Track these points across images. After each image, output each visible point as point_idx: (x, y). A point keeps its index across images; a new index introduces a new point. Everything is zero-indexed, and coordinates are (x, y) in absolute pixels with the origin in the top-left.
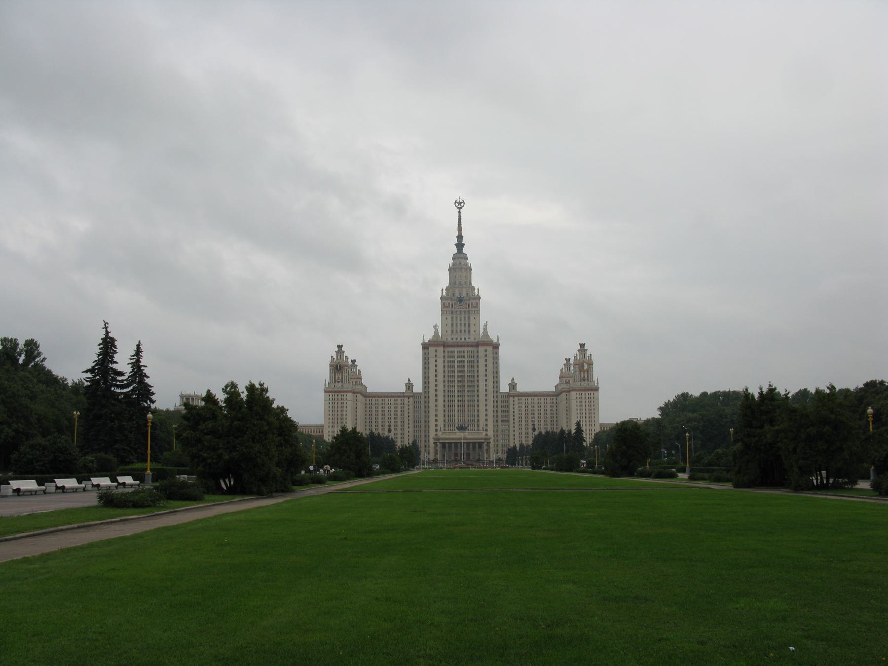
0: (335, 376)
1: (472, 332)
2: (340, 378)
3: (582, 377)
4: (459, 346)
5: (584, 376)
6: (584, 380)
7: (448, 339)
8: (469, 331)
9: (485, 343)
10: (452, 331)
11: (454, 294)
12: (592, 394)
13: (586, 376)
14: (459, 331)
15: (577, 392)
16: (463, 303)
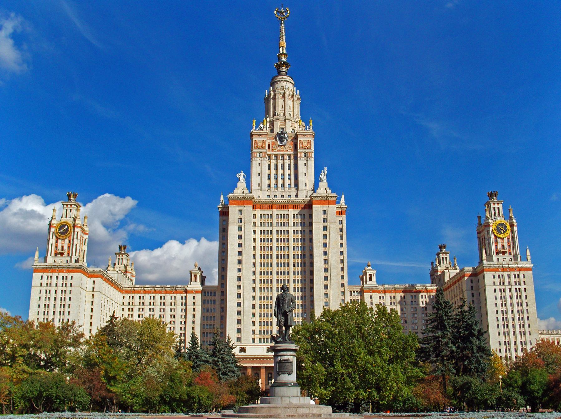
0: (57, 242)
1: (301, 185)
2: (66, 247)
3: (500, 246)
4: (278, 207)
5: (503, 246)
6: (504, 253)
7: (262, 196)
8: (296, 185)
9: (323, 199)
10: (269, 185)
11: (272, 131)
12: (521, 276)
13: (506, 246)
14: (279, 185)
15: (494, 273)
16: (285, 141)
